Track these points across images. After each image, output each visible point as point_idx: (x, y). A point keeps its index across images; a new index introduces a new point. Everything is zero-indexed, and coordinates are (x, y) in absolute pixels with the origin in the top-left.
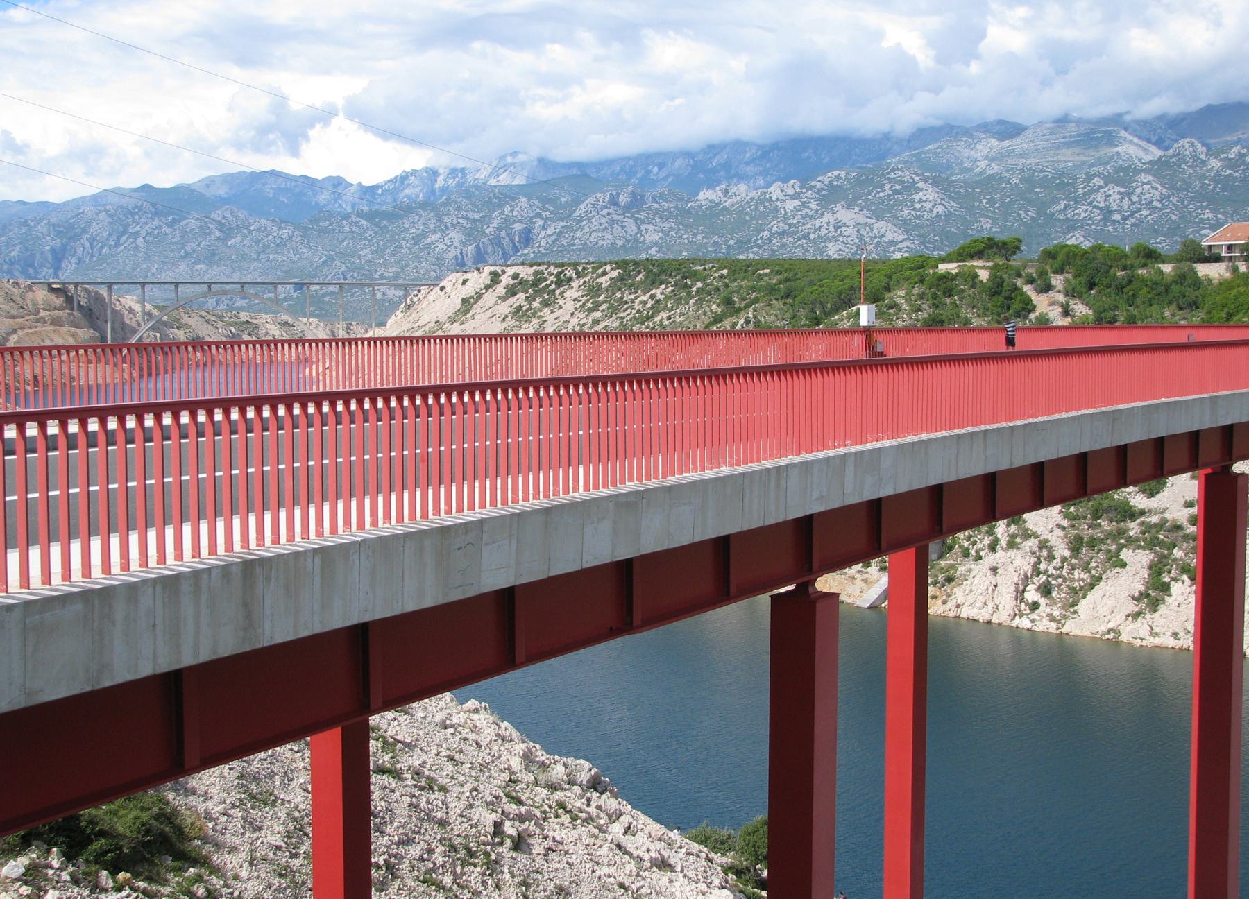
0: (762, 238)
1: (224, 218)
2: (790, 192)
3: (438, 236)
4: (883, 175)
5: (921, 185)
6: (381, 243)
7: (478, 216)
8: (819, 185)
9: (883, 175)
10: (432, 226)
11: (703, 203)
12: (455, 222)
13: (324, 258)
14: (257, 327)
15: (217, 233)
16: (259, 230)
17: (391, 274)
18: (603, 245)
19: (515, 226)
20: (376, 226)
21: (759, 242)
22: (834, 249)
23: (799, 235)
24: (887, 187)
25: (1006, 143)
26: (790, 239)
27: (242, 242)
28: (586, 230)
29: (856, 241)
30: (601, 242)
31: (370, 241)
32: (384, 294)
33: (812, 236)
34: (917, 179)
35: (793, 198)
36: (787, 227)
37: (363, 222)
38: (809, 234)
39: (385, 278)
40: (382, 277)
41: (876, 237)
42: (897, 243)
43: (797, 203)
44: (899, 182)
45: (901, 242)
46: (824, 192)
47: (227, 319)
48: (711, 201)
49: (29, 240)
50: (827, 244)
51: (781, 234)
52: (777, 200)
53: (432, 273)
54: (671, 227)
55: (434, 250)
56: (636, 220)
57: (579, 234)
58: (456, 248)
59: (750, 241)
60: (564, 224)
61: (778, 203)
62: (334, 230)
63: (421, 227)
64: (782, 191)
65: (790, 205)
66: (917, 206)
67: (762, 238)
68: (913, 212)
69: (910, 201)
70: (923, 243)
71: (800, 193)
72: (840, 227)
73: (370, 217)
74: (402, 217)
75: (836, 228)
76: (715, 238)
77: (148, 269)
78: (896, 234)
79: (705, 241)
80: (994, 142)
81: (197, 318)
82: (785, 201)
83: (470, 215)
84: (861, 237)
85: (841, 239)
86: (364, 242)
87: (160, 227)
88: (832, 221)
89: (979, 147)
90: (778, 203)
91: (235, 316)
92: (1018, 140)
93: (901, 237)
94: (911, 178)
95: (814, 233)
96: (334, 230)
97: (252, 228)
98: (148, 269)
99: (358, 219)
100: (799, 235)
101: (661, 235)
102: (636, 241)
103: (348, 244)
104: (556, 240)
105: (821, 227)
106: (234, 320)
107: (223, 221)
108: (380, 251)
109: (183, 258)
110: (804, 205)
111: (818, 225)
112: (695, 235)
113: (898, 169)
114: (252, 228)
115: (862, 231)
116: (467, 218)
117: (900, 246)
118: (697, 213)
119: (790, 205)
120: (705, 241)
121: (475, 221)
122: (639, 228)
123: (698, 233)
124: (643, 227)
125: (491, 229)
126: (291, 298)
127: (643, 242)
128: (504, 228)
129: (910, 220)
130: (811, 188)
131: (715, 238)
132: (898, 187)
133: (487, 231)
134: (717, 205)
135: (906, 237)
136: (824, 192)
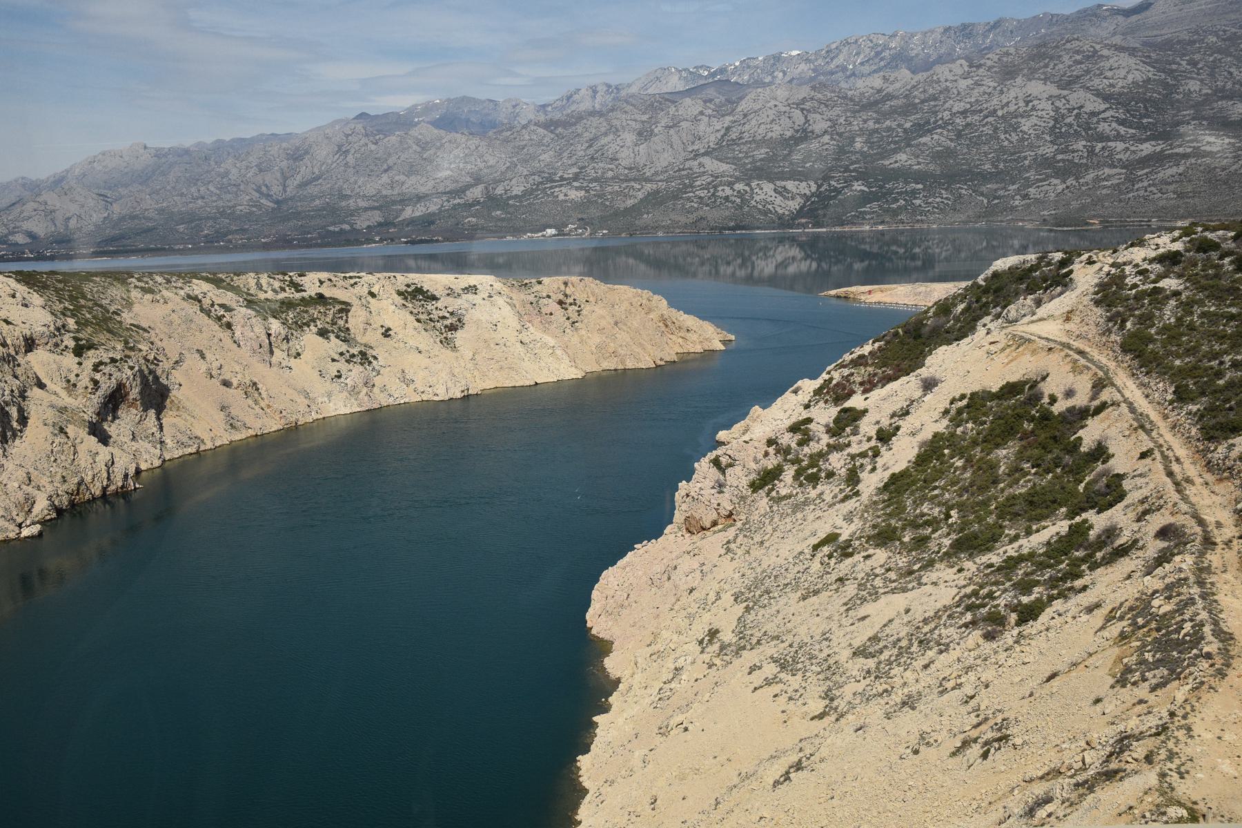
0: (942, 119)
1: (420, 134)
2: (960, 72)
3: (611, 137)
4: (1057, 47)
5: (1105, 52)
7: (645, 118)
8: (989, 63)
9: (1057, 47)
10: (603, 130)
11: (865, 90)
12: (624, 124)
13: (508, 164)
14: (345, 308)
15: (415, 147)
16: (450, 141)
18: (771, 138)
19: (682, 124)
20: (552, 132)
21: (940, 122)
22: (1029, 124)
23: (986, 112)
24: (1066, 58)
25: (1134, 18)
26: (976, 117)
27: (435, 154)
28: (754, 122)
29: (1052, 114)
30: (770, 135)
31: (548, 146)
32: (566, 195)
33: (1000, 113)
34: (1098, 47)
36: (968, 106)
37: (541, 131)
38: (995, 111)
39: (565, 179)
40: (562, 179)
41: (1074, 109)
42: (1099, 113)
43: (970, 81)
44: (1078, 52)
45: (1104, 111)
46: (995, 69)
48: (872, 88)
50: (1019, 120)
51: (964, 113)
52: (946, 81)
53: (610, 172)
54: (838, 115)
56: (802, 110)
57: (747, 127)
58: (629, 147)
59: (928, 122)
60: (731, 118)
61: (948, 84)
64: (950, 71)
65: (963, 84)
66: (1109, 74)
67: (942, 119)
68: (1104, 80)
69: (1098, 69)
70: (1128, 111)
71: (969, 73)
72: (1031, 101)
74: (575, 124)
75: (1027, 103)
76: (888, 123)
77: (356, 182)
78: (1096, 104)
79: (877, 126)
80: (1120, 18)
82: (956, 81)
83: (638, 117)
84: (1057, 109)
85: (1035, 113)
87: (367, 144)
88: (1021, 95)
89: (1105, 25)
90: (948, 84)
92: (1148, 13)
93: (1103, 107)
94: (1091, 47)
95: (1002, 109)
97: (444, 141)
98: (356, 182)
99: (535, 128)
100: (986, 112)
101: (829, 123)
102: (804, 130)
104: (725, 134)
105: (1008, 103)
106: (290, 294)
108: (559, 155)
109: (386, 171)
110: (977, 84)
111: (1005, 101)
112: (865, 121)
113: (1074, 39)
114: (444, 141)
115: (1058, 104)
116: (635, 120)
117: (1102, 116)
118: (861, 100)
119: (963, 84)
120: (877, 126)
121: (643, 122)
122: (806, 117)
123: (868, 120)
124: (811, 117)
125: (659, 128)
126: (479, 203)
127: (812, 132)
128: (671, 127)
129: (1103, 89)
131: (888, 123)
132: (1078, 57)
133: (656, 131)
134: (879, 91)
135: (1107, 105)
136: (995, 69)
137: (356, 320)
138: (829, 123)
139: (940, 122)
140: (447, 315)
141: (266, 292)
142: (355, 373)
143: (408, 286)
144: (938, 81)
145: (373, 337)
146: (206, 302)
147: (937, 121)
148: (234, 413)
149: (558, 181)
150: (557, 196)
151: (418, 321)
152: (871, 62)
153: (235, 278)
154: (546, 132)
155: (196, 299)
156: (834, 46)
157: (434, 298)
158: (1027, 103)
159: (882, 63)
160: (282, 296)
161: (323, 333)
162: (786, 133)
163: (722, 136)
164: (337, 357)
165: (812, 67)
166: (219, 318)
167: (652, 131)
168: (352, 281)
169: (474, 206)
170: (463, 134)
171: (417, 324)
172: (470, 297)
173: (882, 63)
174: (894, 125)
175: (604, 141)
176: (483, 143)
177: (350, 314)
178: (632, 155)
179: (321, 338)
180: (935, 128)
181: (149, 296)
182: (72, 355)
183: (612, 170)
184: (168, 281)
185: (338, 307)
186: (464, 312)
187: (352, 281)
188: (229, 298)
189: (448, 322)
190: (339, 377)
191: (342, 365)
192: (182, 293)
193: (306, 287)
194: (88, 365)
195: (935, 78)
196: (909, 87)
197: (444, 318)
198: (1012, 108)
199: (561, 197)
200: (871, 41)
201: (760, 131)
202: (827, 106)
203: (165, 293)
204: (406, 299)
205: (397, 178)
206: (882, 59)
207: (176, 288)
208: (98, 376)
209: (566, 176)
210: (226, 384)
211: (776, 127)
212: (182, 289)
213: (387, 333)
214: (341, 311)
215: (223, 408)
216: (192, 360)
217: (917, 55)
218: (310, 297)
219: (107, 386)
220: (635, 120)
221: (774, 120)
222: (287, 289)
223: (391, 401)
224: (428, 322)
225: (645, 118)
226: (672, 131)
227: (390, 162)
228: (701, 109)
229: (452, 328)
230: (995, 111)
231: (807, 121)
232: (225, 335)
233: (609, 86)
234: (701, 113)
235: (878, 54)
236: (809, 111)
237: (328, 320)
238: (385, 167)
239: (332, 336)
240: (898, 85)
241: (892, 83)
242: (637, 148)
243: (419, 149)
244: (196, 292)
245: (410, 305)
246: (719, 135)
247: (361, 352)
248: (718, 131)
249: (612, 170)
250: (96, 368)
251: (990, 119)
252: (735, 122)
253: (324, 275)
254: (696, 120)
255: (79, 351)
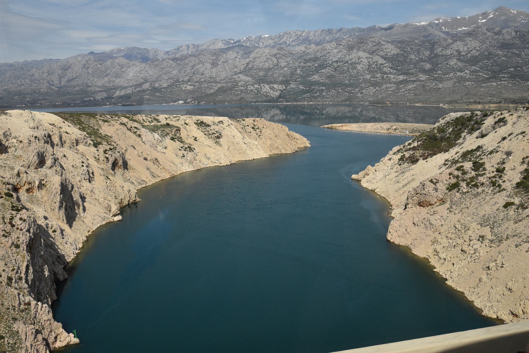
0: (329, 63)
1: (120, 61)
2: (333, 46)
3: (201, 65)
4: (366, 39)
5: (383, 43)
6: (179, 69)
7: (214, 58)
8: (343, 44)
9: (366, 39)
10: (197, 62)
11: (299, 51)
12: (206, 60)
13: (158, 75)
15: (118, 67)
16: (133, 65)
17: (187, 80)
18: (265, 68)
20: (175, 62)
21: (328, 65)
22: (360, 67)
23: (344, 61)
24: (370, 44)
25: (388, 31)
26: (341, 63)
28: (258, 62)
29: (368, 64)
30: (264, 66)
31: (175, 68)
32: (185, 88)
33: (349, 62)
34: (380, 41)
35: (336, 48)
36: (338, 59)
37: (171, 61)
38: (348, 61)
39: (185, 81)
40: (183, 81)
41: (375, 62)
42: (383, 64)
43: (337, 50)
44: (374, 42)
45: (385, 64)
47: (148, 123)
48: (301, 50)
49: (50, 71)
50: (357, 65)
51: (337, 62)
53: (203, 79)
55: (200, 70)
56: (276, 58)
57: (255, 63)
58: (208, 69)
59: (324, 64)
61: (330, 51)
62: (160, 64)
63: (193, 63)
64: (330, 46)
65: (335, 51)
66: (385, 51)
67: (329, 63)
68: (384, 53)
69: (381, 48)
70: (393, 64)
71: (337, 47)
72: (360, 59)
73: (175, 59)
74: (184, 59)
75: (359, 59)
76: (309, 64)
77: (93, 80)
78: (382, 61)
79: (305, 65)
80: (384, 31)
81: (117, 126)
82: (332, 50)
83: (211, 58)
84: (369, 62)
85: (362, 63)
86: (172, 69)
89: (378, 33)
91: (155, 119)
92: (392, 30)
93: (385, 62)
94: (378, 40)
95: (350, 60)
96: (160, 64)
97: (130, 65)
98: (93, 80)
99: (168, 60)
100: (344, 61)
101: (287, 63)
103: (166, 69)
104: (247, 66)
105: (352, 59)
106: (155, 123)
107: (119, 62)
108: (180, 72)
109: (106, 76)
111: (351, 58)
112: (300, 63)
113: (372, 37)
114: (130, 65)
115: (369, 60)
116: (210, 59)
117: (384, 65)
119: (335, 51)
120: (305, 65)
121: (213, 60)
122: (278, 60)
123: (301, 62)
124: (280, 60)
126: (149, 90)
127: (280, 66)
129: (384, 56)
130: (340, 45)
132: (374, 44)
133: (219, 63)
134: (304, 52)
135: (386, 62)
137: (183, 134)
138: (287, 63)
139: (328, 65)
140: (215, 132)
141: (146, 122)
142: (190, 155)
143: (197, 120)
144: (326, 50)
145: (191, 141)
146: (129, 126)
147: (327, 64)
148: (152, 171)
149: (181, 82)
150: (182, 88)
151: (205, 134)
152: (296, 41)
153: (134, 116)
154: (173, 62)
155: (124, 124)
156: (281, 34)
157: (209, 126)
158: (359, 59)
159: (300, 42)
160: (152, 124)
161: (172, 139)
162: (270, 66)
163: (246, 66)
164: (180, 148)
165: (274, 41)
166: (135, 133)
167: (217, 63)
168: (177, 118)
169: (147, 91)
170: (138, 62)
171: (205, 136)
172: (221, 125)
173: (300, 42)
174: (311, 65)
175: (198, 67)
176: (147, 66)
177: (181, 131)
178: (210, 72)
179: (172, 141)
180: (326, 67)
181: (106, 123)
182: (93, 147)
183: (203, 78)
184: (112, 117)
185: (175, 129)
186: (221, 131)
187: (177, 118)
188: (136, 124)
189: (216, 135)
190: (184, 156)
191: (183, 152)
192: (118, 122)
193: (161, 120)
194: (101, 150)
195: (325, 48)
196: (315, 51)
197: (214, 133)
198: (354, 61)
199: (184, 88)
200: (295, 33)
201: (260, 65)
202: (285, 57)
203: (112, 122)
204: (198, 126)
205: (111, 79)
206: (300, 40)
207: (116, 120)
208: (107, 155)
209: (184, 80)
210: (146, 159)
211: (266, 64)
212: (118, 120)
213: (195, 139)
214: (177, 130)
215: (148, 169)
216: (130, 150)
217: (312, 39)
218: (164, 124)
219: (112, 160)
220: (210, 59)
221: (265, 61)
222: (154, 121)
223: (204, 166)
224: (209, 135)
225: (214, 58)
226: (225, 64)
227: (108, 72)
228: (236, 56)
229: (218, 137)
230: (348, 61)
231: (278, 62)
232: (139, 139)
233: (194, 45)
234: (236, 57)
235: (298, 38)
236: (278, 58)
237: (173, 134)
238: (105, 74)
239: (176, 140)
240: (311, 50)
241: (309, 49)
242: (212, 70)
243: (120, 68)
244: (124, 122)
245: (200, 128)
246: (244, 66)
247: (188, 147)
248: (244, 64)
249: (203, 78)
250: (105, 152)
251: (346, 64)
252: (250, 61)
253: (166, 116)
254: (234, 60)
255: (95, 145)
